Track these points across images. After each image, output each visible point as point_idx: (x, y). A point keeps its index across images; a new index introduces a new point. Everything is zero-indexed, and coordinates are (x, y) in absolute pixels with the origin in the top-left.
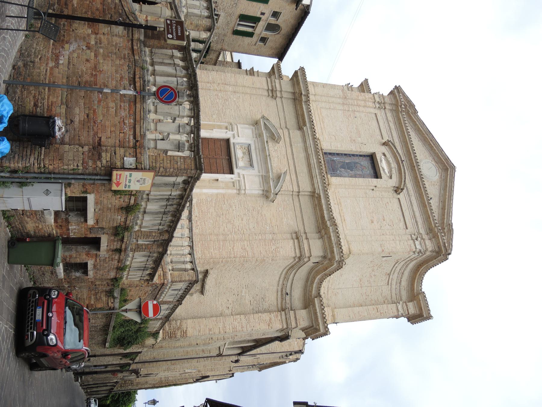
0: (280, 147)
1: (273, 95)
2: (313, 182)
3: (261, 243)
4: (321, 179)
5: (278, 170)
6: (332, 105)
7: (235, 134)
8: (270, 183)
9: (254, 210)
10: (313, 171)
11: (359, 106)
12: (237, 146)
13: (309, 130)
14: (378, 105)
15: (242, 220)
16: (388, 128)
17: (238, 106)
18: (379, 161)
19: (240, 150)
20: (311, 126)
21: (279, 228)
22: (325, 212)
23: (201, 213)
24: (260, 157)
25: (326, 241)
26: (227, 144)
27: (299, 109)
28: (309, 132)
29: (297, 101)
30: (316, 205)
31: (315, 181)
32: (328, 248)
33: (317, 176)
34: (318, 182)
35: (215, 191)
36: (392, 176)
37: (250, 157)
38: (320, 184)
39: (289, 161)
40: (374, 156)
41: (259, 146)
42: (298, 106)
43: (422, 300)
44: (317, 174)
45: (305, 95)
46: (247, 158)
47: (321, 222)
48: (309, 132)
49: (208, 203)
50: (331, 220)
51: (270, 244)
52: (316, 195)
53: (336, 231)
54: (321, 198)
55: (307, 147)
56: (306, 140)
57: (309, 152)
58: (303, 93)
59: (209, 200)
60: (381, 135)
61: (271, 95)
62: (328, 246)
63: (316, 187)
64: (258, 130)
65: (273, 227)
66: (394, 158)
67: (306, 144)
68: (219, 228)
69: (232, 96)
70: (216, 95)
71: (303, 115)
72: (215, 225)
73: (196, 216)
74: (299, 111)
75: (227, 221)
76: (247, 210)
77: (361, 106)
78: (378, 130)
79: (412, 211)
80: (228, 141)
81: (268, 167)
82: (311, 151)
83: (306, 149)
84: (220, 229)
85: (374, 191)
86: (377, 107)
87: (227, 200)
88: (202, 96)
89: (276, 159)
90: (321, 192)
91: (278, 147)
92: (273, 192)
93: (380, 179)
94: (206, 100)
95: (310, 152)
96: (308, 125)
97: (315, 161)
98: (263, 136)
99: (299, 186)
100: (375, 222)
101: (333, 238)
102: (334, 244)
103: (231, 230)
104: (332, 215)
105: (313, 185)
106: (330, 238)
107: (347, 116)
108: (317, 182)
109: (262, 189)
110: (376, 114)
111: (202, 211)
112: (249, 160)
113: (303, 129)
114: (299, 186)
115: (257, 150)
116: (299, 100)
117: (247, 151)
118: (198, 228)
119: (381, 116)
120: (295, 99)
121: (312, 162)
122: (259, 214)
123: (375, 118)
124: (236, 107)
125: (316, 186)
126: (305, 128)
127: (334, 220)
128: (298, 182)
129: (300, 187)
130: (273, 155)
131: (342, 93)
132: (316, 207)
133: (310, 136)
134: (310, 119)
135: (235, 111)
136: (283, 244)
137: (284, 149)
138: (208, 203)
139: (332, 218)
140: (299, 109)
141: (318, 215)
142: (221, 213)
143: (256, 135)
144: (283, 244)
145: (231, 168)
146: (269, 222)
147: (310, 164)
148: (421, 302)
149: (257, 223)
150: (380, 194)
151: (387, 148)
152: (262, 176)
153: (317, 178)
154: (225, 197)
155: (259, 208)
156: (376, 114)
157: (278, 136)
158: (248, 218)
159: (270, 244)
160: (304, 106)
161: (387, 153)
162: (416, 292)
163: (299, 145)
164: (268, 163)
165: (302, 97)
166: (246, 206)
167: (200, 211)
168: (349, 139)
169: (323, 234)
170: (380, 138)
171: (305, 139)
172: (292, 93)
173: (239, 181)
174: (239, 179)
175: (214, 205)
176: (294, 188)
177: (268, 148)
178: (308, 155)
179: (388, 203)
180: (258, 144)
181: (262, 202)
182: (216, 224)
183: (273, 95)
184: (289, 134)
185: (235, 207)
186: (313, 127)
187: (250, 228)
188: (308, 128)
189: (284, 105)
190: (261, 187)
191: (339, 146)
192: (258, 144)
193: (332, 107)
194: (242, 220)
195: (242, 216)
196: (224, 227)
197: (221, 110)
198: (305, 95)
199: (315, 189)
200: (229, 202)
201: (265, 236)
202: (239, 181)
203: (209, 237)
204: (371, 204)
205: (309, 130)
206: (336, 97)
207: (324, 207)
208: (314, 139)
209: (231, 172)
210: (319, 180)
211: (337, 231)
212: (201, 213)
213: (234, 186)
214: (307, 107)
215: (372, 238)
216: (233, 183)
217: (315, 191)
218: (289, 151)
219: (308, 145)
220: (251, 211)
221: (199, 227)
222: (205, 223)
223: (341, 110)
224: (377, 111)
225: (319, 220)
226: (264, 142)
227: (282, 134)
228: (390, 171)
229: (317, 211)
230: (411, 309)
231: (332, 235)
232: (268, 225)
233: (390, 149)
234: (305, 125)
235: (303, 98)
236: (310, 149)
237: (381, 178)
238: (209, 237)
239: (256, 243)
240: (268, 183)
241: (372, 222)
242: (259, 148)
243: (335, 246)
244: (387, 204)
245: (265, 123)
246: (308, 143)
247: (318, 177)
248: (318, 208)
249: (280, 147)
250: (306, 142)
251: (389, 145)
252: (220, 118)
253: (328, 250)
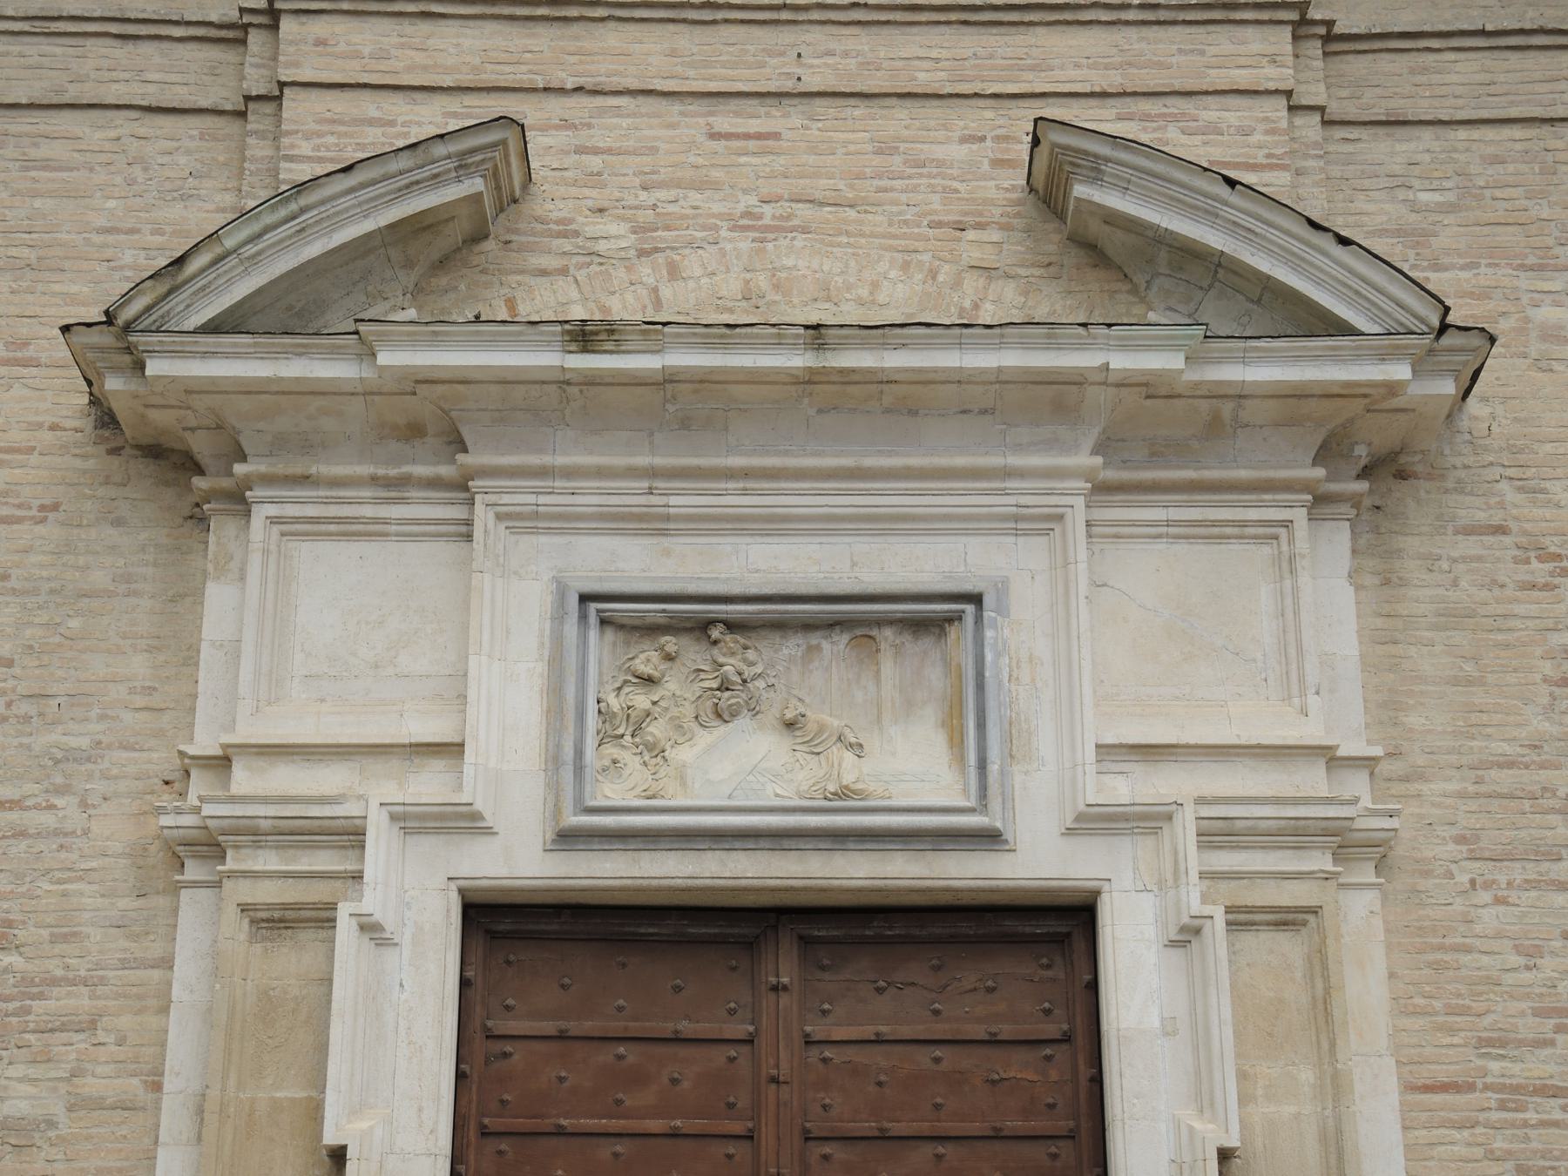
0: (595, 178)
5: (975, 255)
7: (390, 791)
8: (1240, 395)
12: (611, 792)
19: (682, 754)
24: (730, 474)
37: (780, 626)
39: (813, 82)
41: (601, 473)
64: (308, 445)
81: (1001, 379)
87: (1495, 1043)
91: (595, 196)
92: (1400, 371)
98: (463, 379)
109: (1301, 515)
112: (834, 646)
115: (682, 502)
117: (692, 653)
130: (731, 286)
143: (404, 482)
152: (1102, 490)
154: (1442, 1073)
157: (463, 166)
164: (925, 379)
173: (1215, 835)
174: (1186, 828)
180: (570, 473)
190: (1270, 532)
192: (570, 473)
200: (1529, 1027)
202: (1215, 835)
213: (1288, 919)
216: (1241, 920)
226: (564, 381)
242: (653, 473)
245: (213, 328)
249: (595, 178)
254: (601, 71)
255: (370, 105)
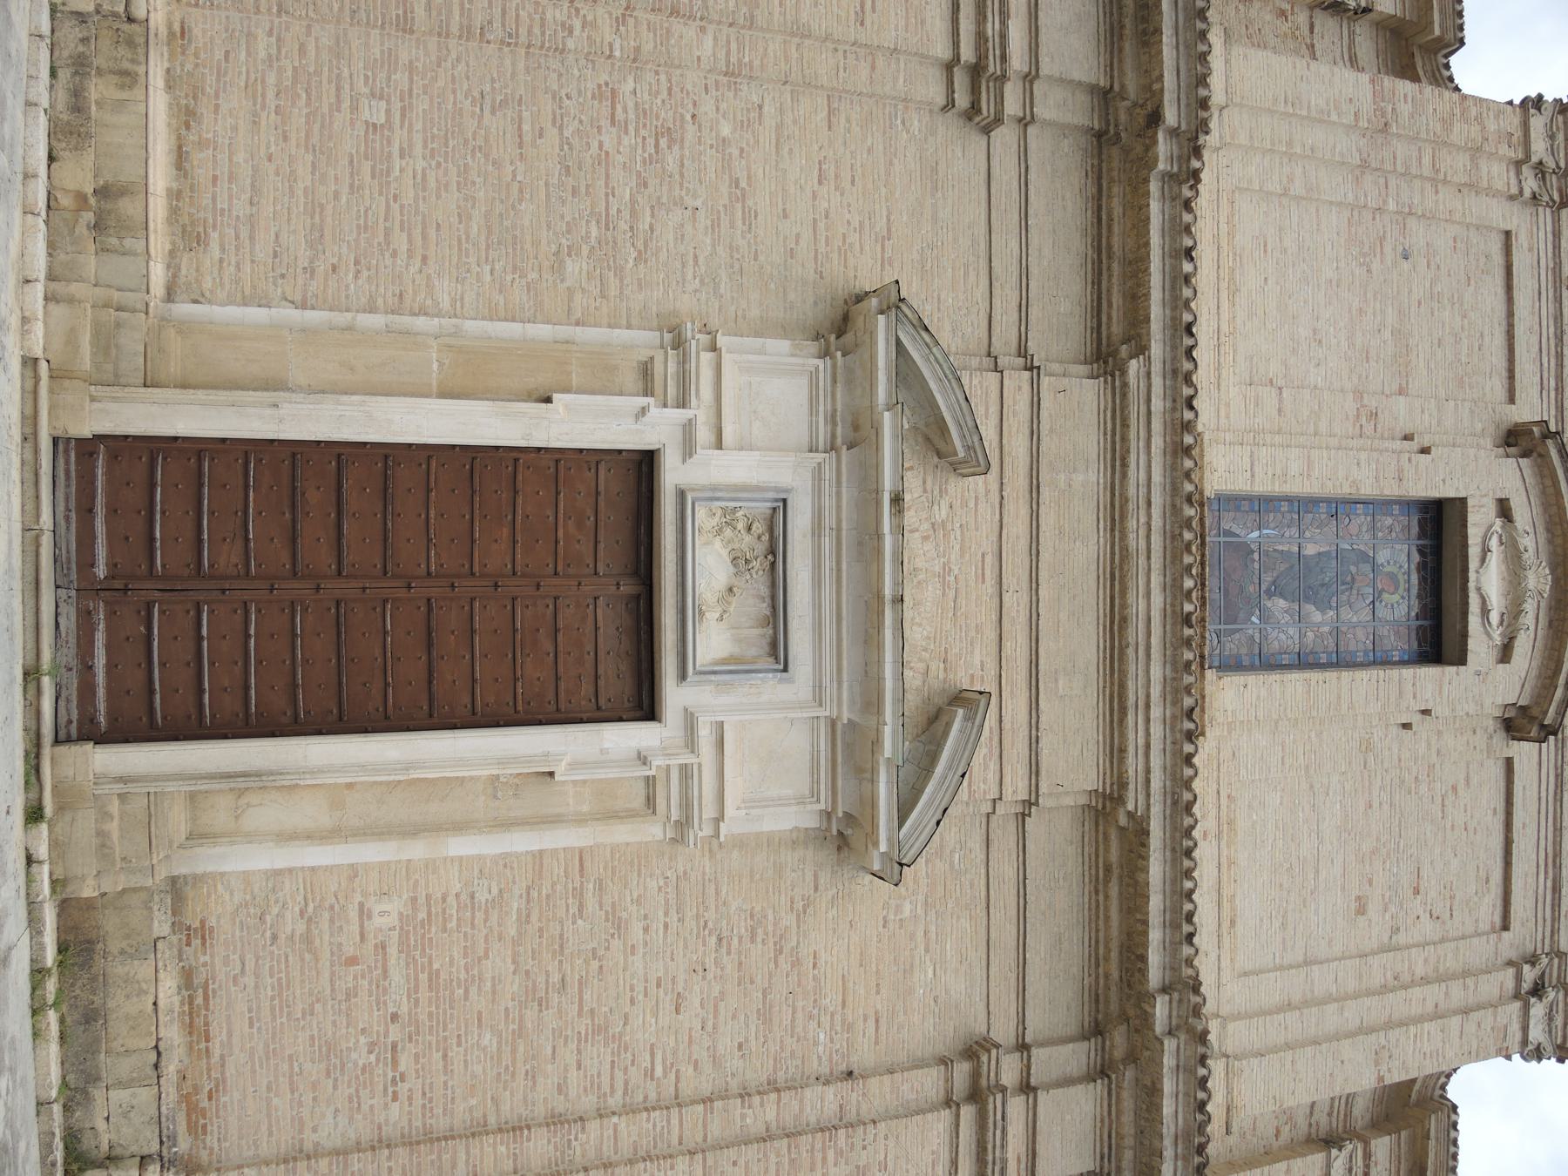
0: (965, 504)
1: (975, 108)
2: (1123, 735)
3: (773, 1159)
4: (1171, 723)
5: (933, 667)
6: (1298, 171)
7: (701, 419)
8: (873, 781)
9: (753, 939)
10: (1132, 668)
11: (1437, 181)
12: (701, 513)
13: (1157, 381)
14: (1531, 184)
15: (677, 1011)
16: (1552, 330)
17: (743, 184)
18: (1474, 551)
19: (718, 543)
20: (1174, 359)
21: (883, 1029)
22: (1155, 935)
23: (424, 994)
24: (839, 563)
25: (1128, 1104)
26: (639, 483)
27: (1117, 211)
28: (1157, 404)
29: (1115, 151)
30: (1108, 869)
31: (1131, 736)
32: (1129, 1141)
33: (1148, 706)
34: (1148, 746)
35: (522, 842)
36: (1517, 643)
37: (773, 585)
38: (1156, 762)
39: (1006, 597)
40: (1449, 515)
41: (839, 507)
42: (1115, 190)
43: (1437, 1139)
44: (1156, 691)
45: (1174, 133)
46: (751, 602)
47: (1115, 974)
48: (1157, 404)
49: (479, 916)
50: (1176, 996)
51: (819, 1156)
52: (1123, 820)
53: (1193, 1072)
54: (1145, 845)
55: (1125, 500)
56: (1126, 452)
57: (1132, 536)
58: (1170, 116)
59: (482, 897)
60: (1505, 374)
61: (962, 101)
62: (1128, 1129)
63: (1131, 772)
64: (849, 382)
65: (849, 1027)
66: (1548, 530)
67: (1124, 475)
68: (531, 1076)
69: (707, 107)
70: (598, 95)
71: (1137, 266)
72: (506, 1059)
73: (395, 1017)
74: (1116, 229)
75: (583, 1025)
76: (714, 940)
77: (1445, 182)
78: (1499, 339)
79: (1551, 829)
80: (645, 464)
81: (880, 679)
82: (1142, 532)
83: (1115, 514)
84: (540, 1080)
85: (1407, 734)
86: (1527, 193)
87: (600, 887)
88: (504, 103)
89: (931, 592)
90: (1156, 810)
91: (957, 504)
92: (883, 848)
93: (1453, 669)
94: (527, 138)
95: (1136, 541)
96: (1156, 349)
97: (1157, 600)
98: (878, 448)
99: (1035, 770)
100: (1373, 909)
101: (1168, 1108)
102: (1168, 1142)
103: (605, 1080)
104: (1189, 962)
105: (1116, 752)
106: (1150, 1094)
107: (1366, 249)
108: (1141, 741)
109: (822, 806)
110: (1508, 234)
111: (434, 977)
112: (764, 608)
113: (1124, 372)
114: (1035, 770)
115: (827, 542)
116: (1126, 151)
117: (761, 548)
118: (403, 1096)
119: (1530, 250)
120: (1101, 139)
121: (1137, 605)
122: (781, 959)
123: (1498, 259)
124: (724, 189)
125: (1133, 765)
126: (1133, 365)
127: (1195, 999)
128: (1034, 742)
129: (1043, 773)
130: (920, 563)
131: (1369, 96)
132: (1107, 881)
133: (1157, 425)
134: (1174, 308)
135: (715, 225)
136: (892, 1144)
137: (988, 514)
138: (479, 916)
139: (1186, 986)
140: (1117, 211)
141: (1107, 927)
142: (555, 978)
143: (834, 424)
144: (892, 1144)
145: (645, 665)
146: (831, 1000)
147: (1124, 620)
148: (1432, 1143)
149: (765, 1016)
150: (1433, 742)
151: (1527, 472)
152: (833, 723)
153: (1148, 720)
154: (587, 864)
155: (789, 920)
156: (1508, 234)
157: (968, 448)
158: (716, 991)
159: (819, 1156)
160: (1155, 207)
161: (1523, 515)
162: (1419, 1092)
163: (1079, 478)
164: (880, 647)
165: (1155, 142)
166: (711, 915)
167: (423, 977)
168: (1350, 405)
169: (1118, 1054)
170: (1498, 386)
171: (1124, 439)
172: (1093, 89)
173: (685, 771)
174: (688, 759)
175: (513, 932)
176: (1007, 779)
177: (895, 542)
178: (1125, 556)
179: (1454, 788)
180: (839, 494)
181: (809, 877)
182: (514, 1051)
183: (975, 108)
184: (1036, 404)
185: (646, 930)
186: (1187, 366)
187: (721, 1050)
188: (1156, 368)
189: (1032, 176)
190: (815, 794)
191: (1295, 467)
192: (839, 494)
193: (1298, 188)
194: (677, 1011)
195: (681, 978)
196: (566, 1070)
197: (626, 214)
198: (1174, 133)
199: (1123, 785)
200: (607, 900)
201: (801, 1101)
203: (462, 1156)
204: (1376, 804)
205: (1157, 381)
206: (1335, 123)
207: (1155, 903)
208: (1175, 453)
209: (646, 707)
210: (1156, 730)
211: (1202, 1072)
212: (424, 994)
213: (650, 801)
214: (1173, 219)
215: (1346, 1014)
216: (650, 782)
217: (1121, 800)
218: (1018, 527)
219: (1132, 491)
220: (735, 941)
221: (406, 1086)
222: (445, 1056)
223: (1340, 204)
224: (1517, 219)
225: (1107, 959)
226: (878, 491)
227: (993, 420)
228: (1514, 613)
229: (1107, 909)
230: (1379, 1168)
231: (1168, 1086)
232: (826, 1020)
233: (1542, 477)
234: (1142, 350)
235: (1164, 147)
236: (1143, 520)
237: (1461, 660)
238: (462, 1156)
239: (742, 1162)
240: (864, 773)
241: (1361, 911)
242: (839, 530)
243: (1168, 1153)
244: (1451, 797)
245: (899, 343)
246: (1136, 474)
247: (1156, 712)
248: (1114, 890)
249: (965, 504)
250: (1124, 465)
251: (1544, 456)
252: (613, 283)
253: (1128, 1155)
254: (1010, 506)
255: (994, 409)
